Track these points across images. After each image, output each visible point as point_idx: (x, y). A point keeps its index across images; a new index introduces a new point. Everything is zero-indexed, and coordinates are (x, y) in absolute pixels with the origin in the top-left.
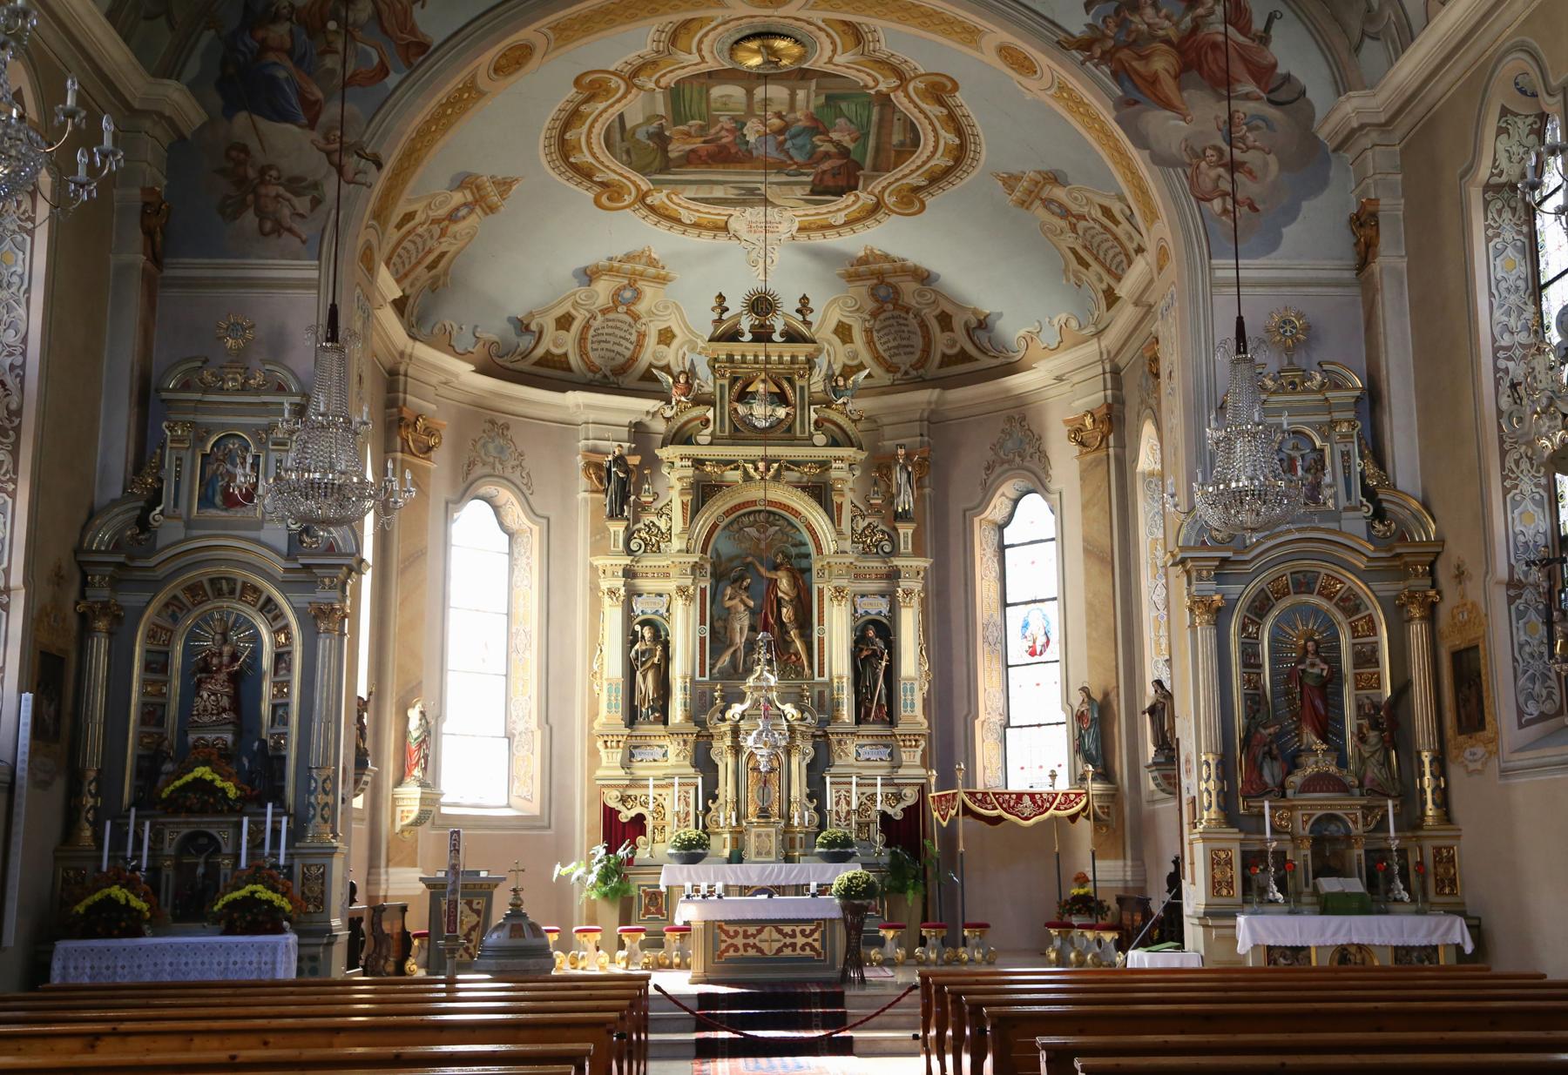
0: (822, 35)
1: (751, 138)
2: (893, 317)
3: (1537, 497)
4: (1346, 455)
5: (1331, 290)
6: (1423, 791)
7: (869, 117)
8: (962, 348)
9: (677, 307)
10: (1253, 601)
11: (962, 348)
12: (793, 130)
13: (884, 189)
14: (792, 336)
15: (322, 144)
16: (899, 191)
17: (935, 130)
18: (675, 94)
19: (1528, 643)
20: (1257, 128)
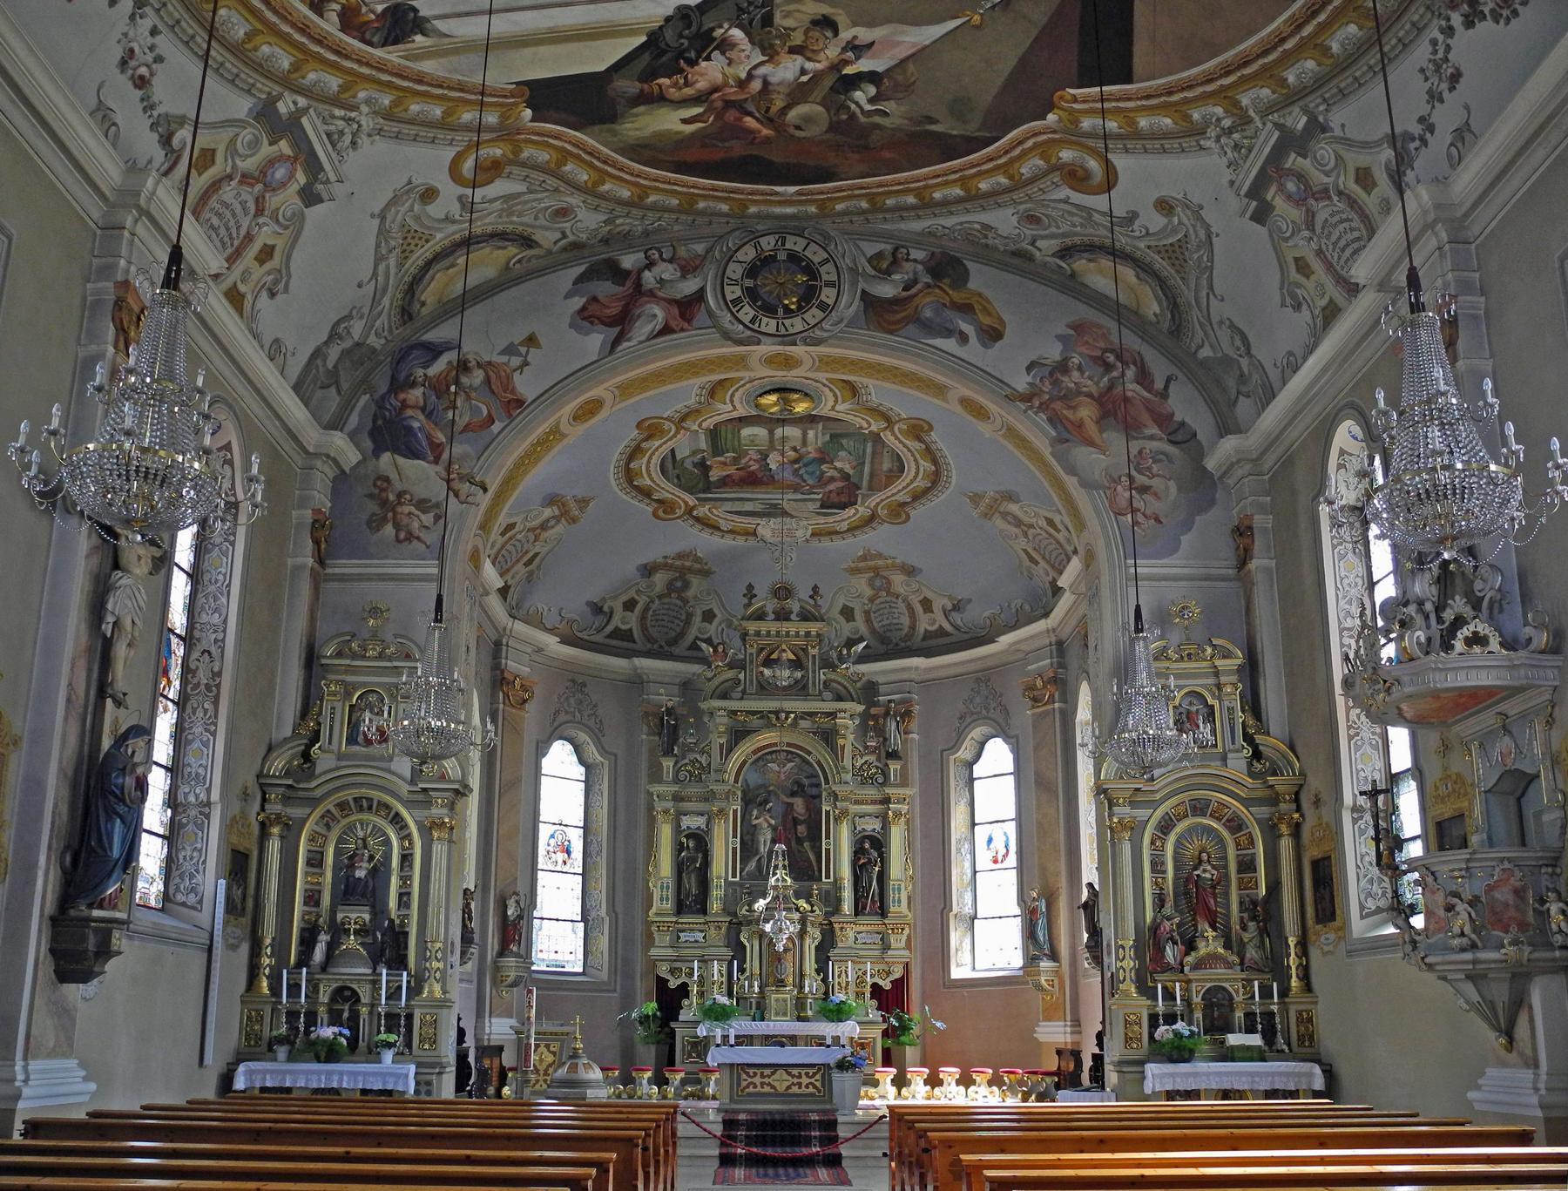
0: (826, 390)
1: (773, 466)
7: (864, 451)
9: (718, 595)
12: (805, 460)
13: (878, 504)
14: (805, 617)
15: (444, 474)
16: (889, 506)
17: (916, 460)
18: (714, 434)
20: (1160, 461)
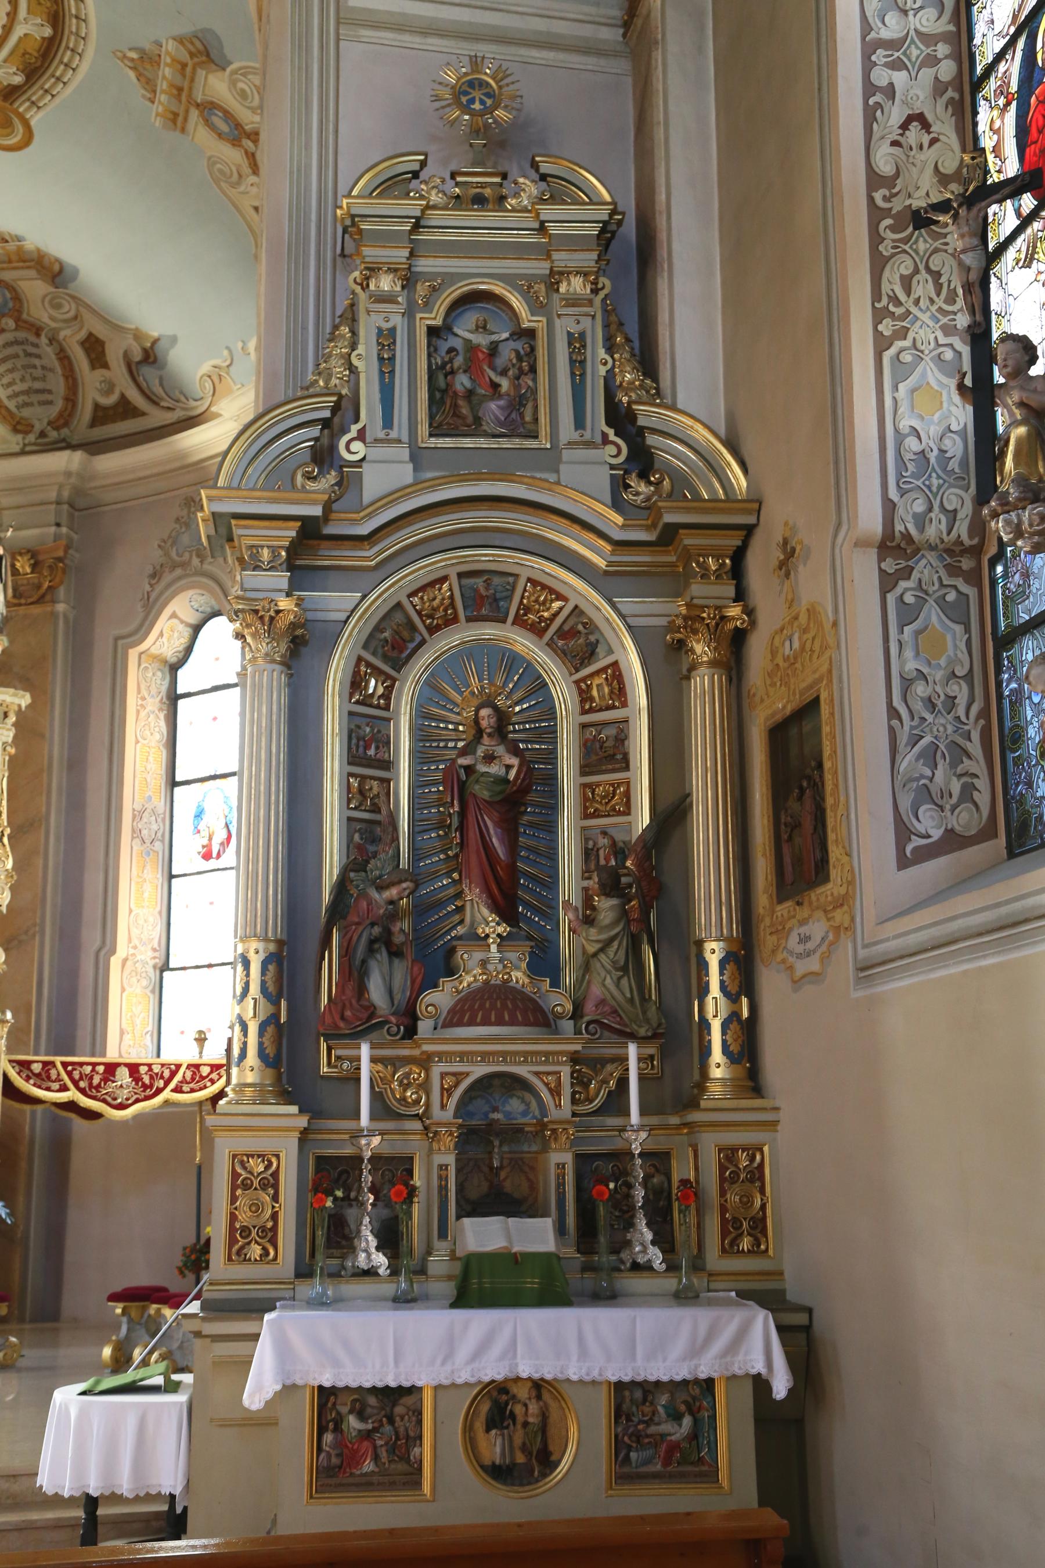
2: (16, 342)
3: (949, 355)
4: (577, 342)
5: (576, 60)
6: (704, 1025)
8: (123, 396)
10: (378, 628)
11: (123, 396)
19: (922, 675)
